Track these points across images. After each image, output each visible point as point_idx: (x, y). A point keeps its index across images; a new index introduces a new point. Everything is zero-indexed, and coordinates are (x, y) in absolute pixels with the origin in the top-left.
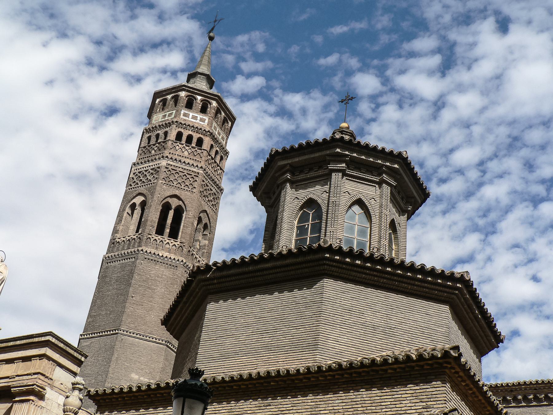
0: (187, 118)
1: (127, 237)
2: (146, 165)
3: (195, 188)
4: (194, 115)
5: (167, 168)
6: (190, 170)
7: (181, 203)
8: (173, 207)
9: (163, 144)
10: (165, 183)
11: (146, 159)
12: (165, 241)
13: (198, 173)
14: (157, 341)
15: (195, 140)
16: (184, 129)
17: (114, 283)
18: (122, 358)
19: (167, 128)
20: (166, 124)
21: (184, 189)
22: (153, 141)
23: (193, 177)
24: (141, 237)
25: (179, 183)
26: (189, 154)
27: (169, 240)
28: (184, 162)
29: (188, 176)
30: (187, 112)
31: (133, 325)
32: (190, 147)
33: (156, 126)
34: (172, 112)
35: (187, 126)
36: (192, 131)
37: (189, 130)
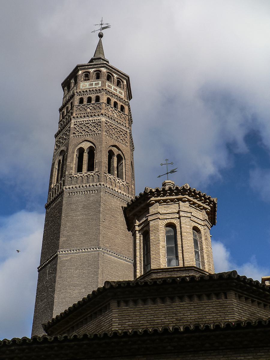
0: (110, 89)
1: (84, 174)
2: (85, 119)
3: (127, 142)
4: (114, 87)
5: (106, 123)
6: (121, 128)
7: (120, 152)
8: (116, 155)
9: (98, 105)
10: (107, 135)
11: (86, 115)
12: (117, 180)
13: (126, 132)
14: (126, 259)
15: (119, 107)
16: (111, 96)
17: (81, 209)
18: (105, 272)
19: (98, 93)
20: (96, 90)
21: (120, 142)
23: (124, 134)
24: (98, 174)
25: (116, 137)
26: (118, 116)
28: (117, 122)
29: (121, 133)
30: (109, 84)
31: (108, 245)
32: (117, 111)
33: (86, 91)
34: (98, 82)
35: (113, 95)
36: (116, 99)
37: (114, 98)
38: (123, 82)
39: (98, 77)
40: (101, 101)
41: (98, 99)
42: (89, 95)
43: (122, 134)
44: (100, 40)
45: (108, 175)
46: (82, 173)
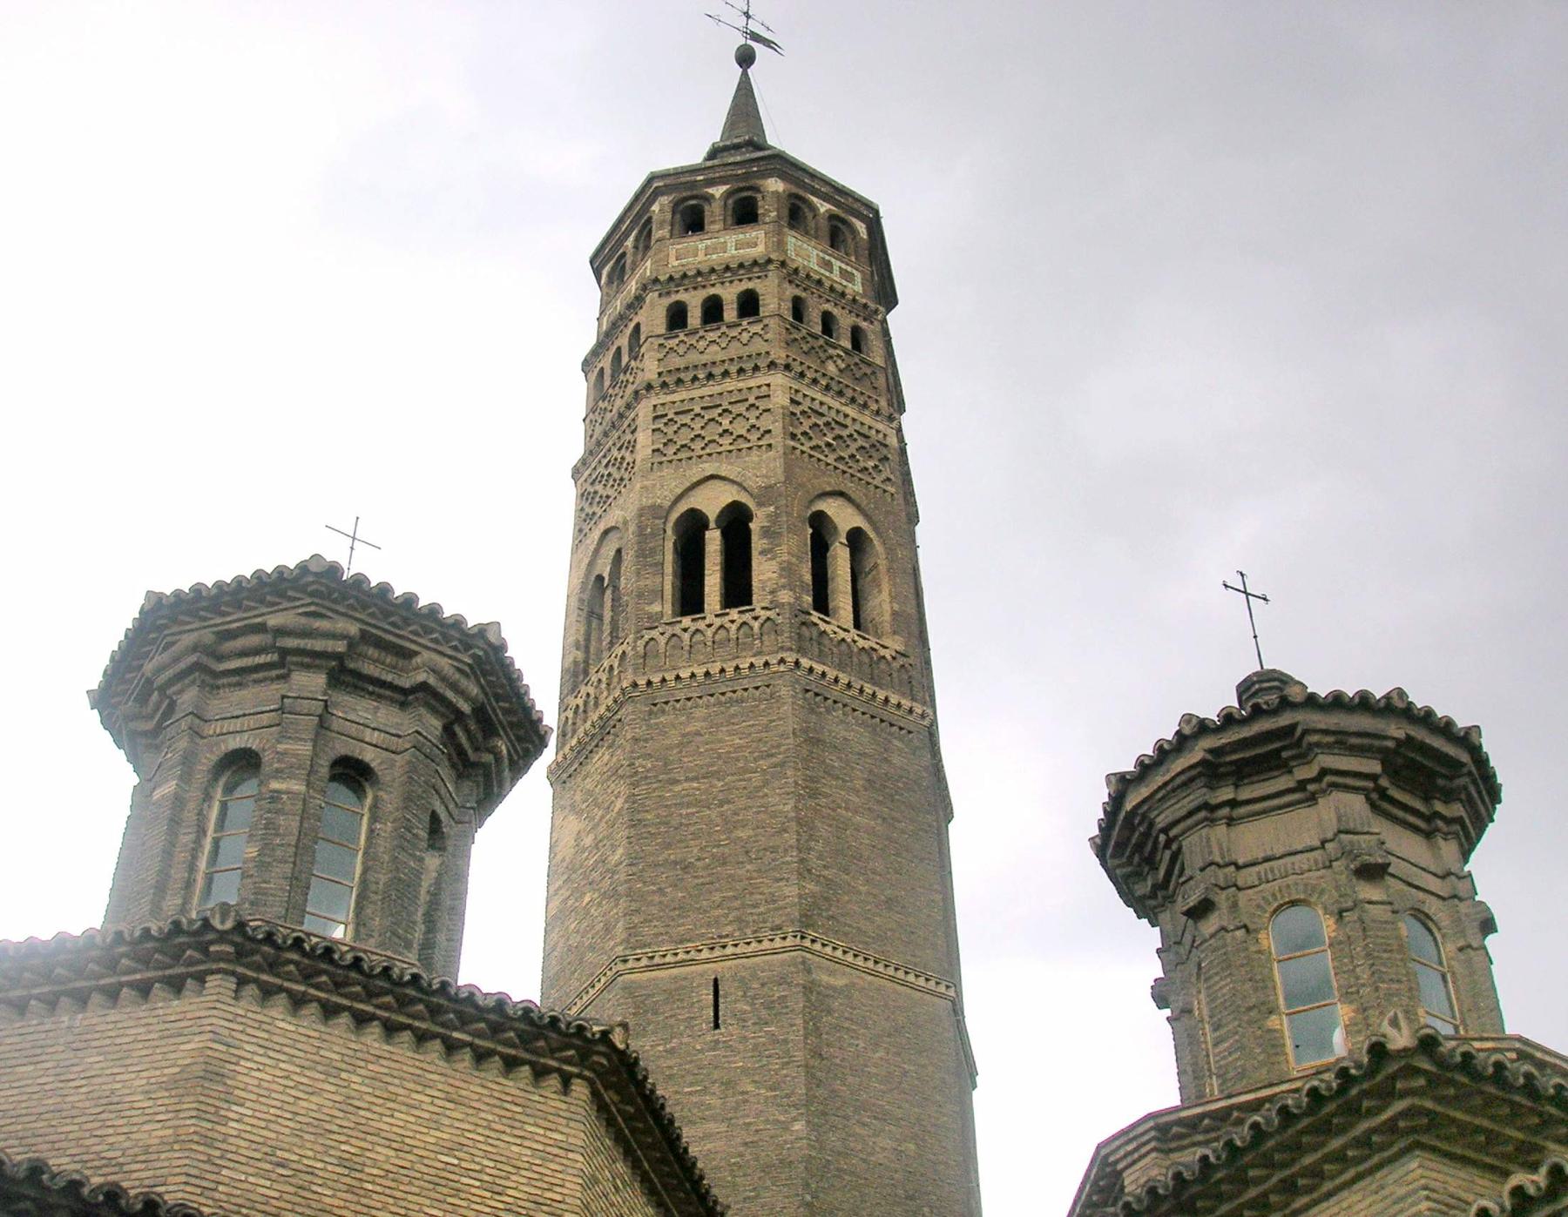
22: (694, 317)
26: (841, 371)
27: (864, 638)
38: (854, 231)
39: (745, 213)
40: (763, 311)
41: (749, 305)
42: (712, 291)
43: (867, 445)
44: (745, 74)
45: (815, 616)
46: (704, 618)
